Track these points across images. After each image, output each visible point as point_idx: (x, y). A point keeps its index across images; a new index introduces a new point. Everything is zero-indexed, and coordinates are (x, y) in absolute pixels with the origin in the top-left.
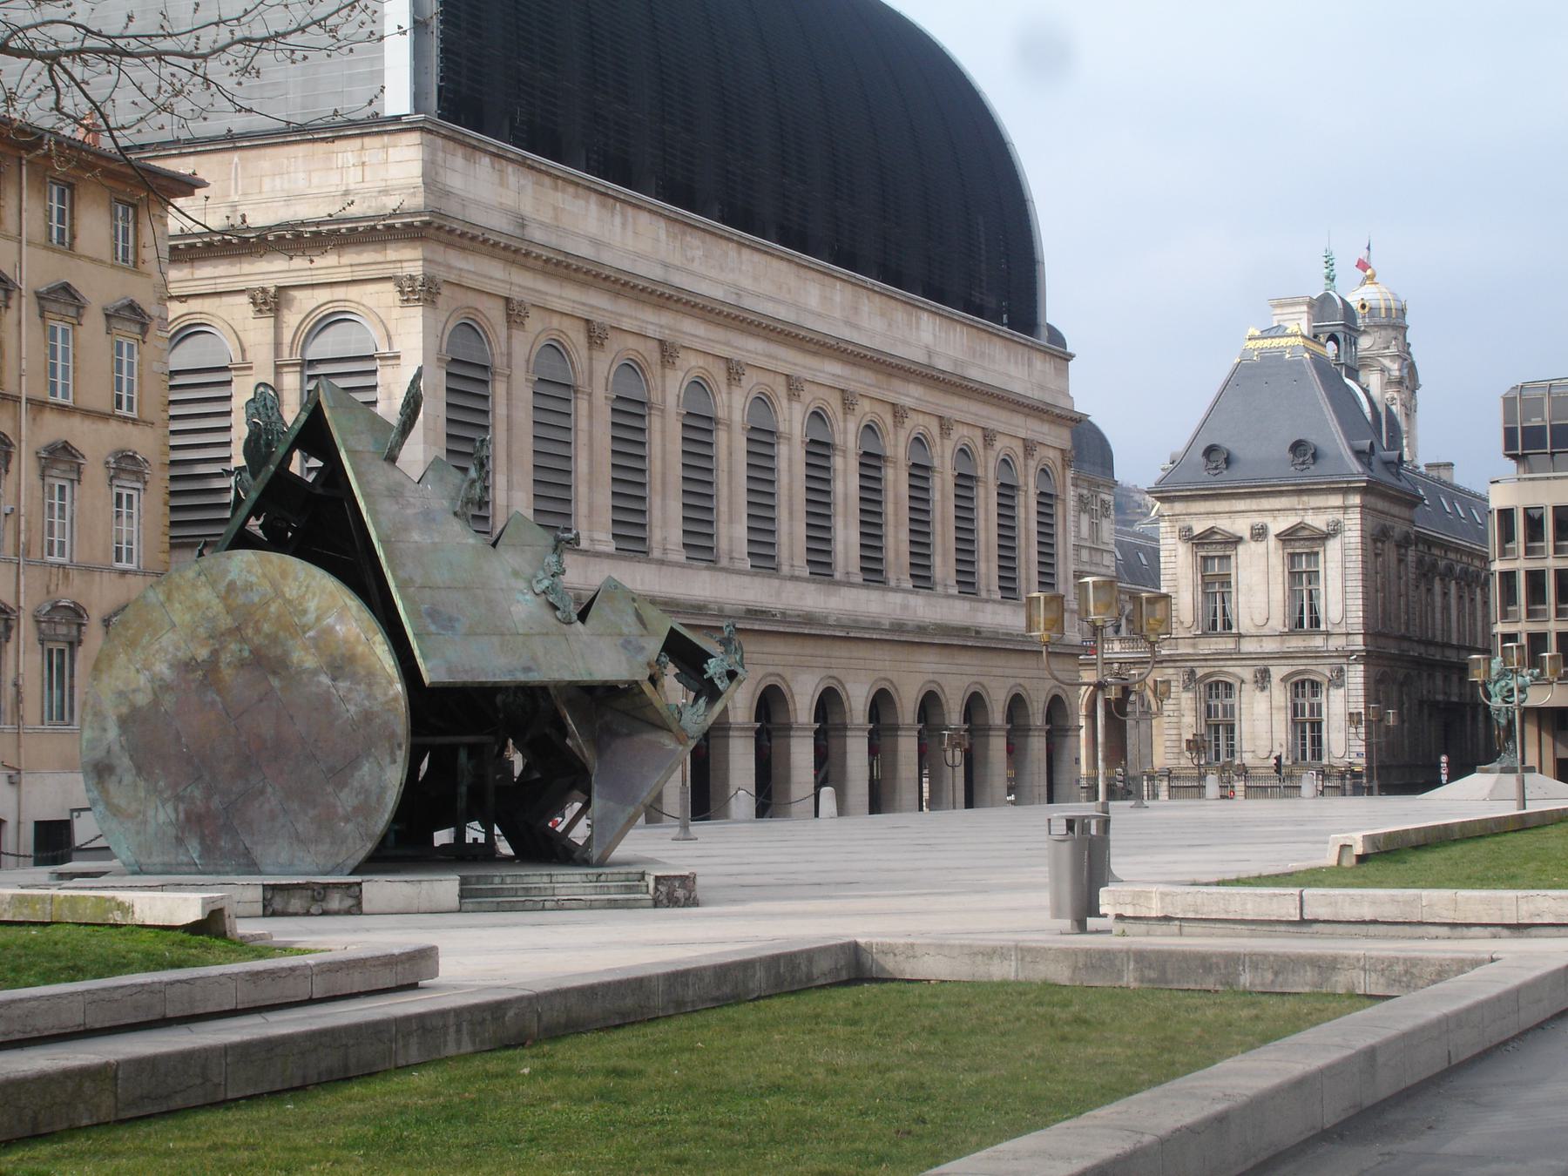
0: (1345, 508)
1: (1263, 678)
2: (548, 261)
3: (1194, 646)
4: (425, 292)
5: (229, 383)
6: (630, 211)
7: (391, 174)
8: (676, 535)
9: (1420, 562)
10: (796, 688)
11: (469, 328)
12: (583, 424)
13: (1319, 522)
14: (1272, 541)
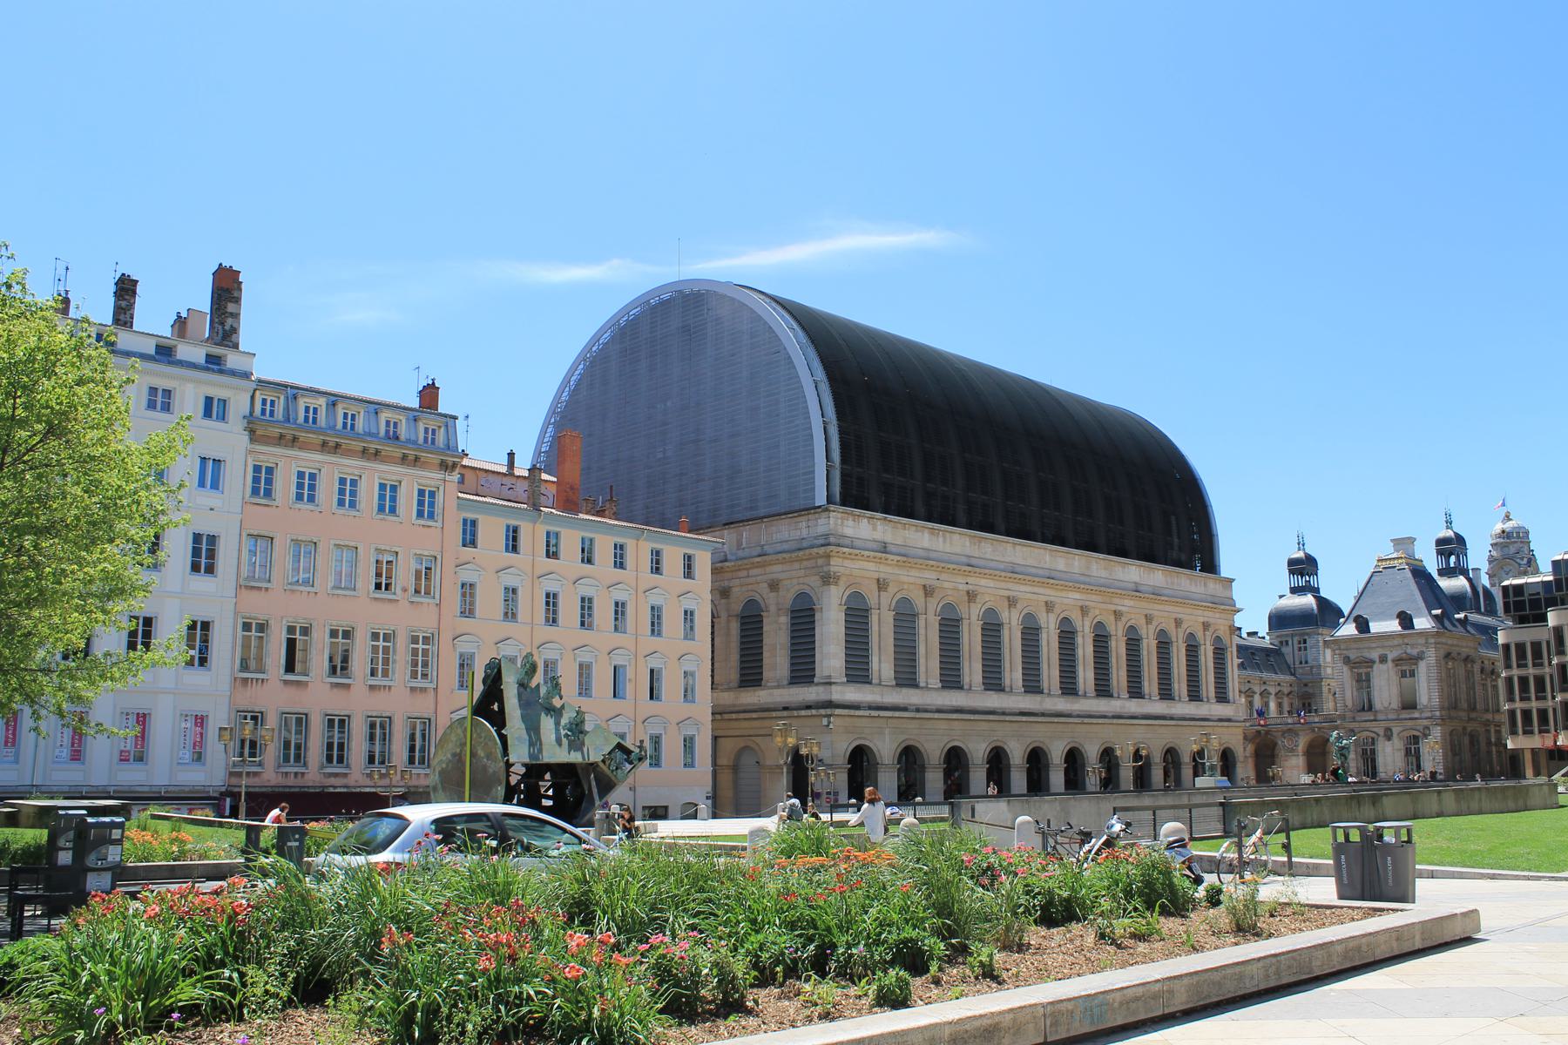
1: (1389, 738)
8: (978, 678)
12: (922, 631)
14: (1390, 664)
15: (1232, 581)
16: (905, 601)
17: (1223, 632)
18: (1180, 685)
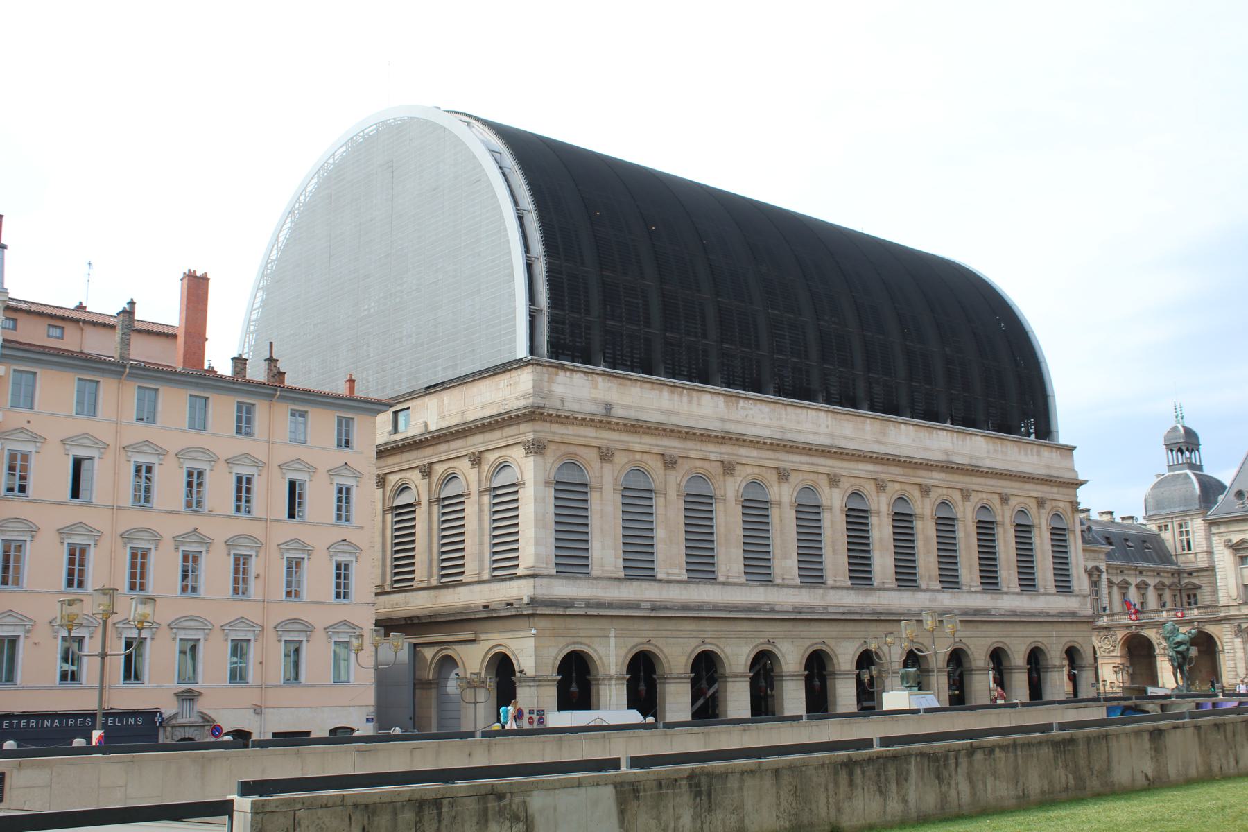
2: (625, 425)
4: (537, 448)
5: (463, 502)
6: (695, 394)
7: (515, 390)
10: (839, 650)
11: (571, 464)
16: (639, 471)
17: (1063, 507)
18: (1008, 573)
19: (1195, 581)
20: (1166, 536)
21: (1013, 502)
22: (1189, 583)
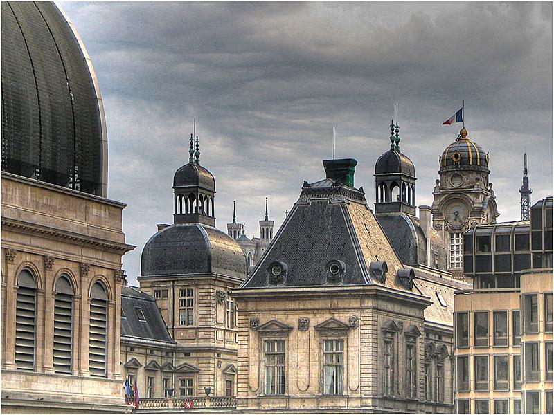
0: (361, 309)
3: (259, 404)
9: (430, 347)
13: (344, 318)
14: (312, 333)
15: (120, 206)
19: (193, 363)
20: (162, 304)
21: (58, 267)
22: (185, 365)
